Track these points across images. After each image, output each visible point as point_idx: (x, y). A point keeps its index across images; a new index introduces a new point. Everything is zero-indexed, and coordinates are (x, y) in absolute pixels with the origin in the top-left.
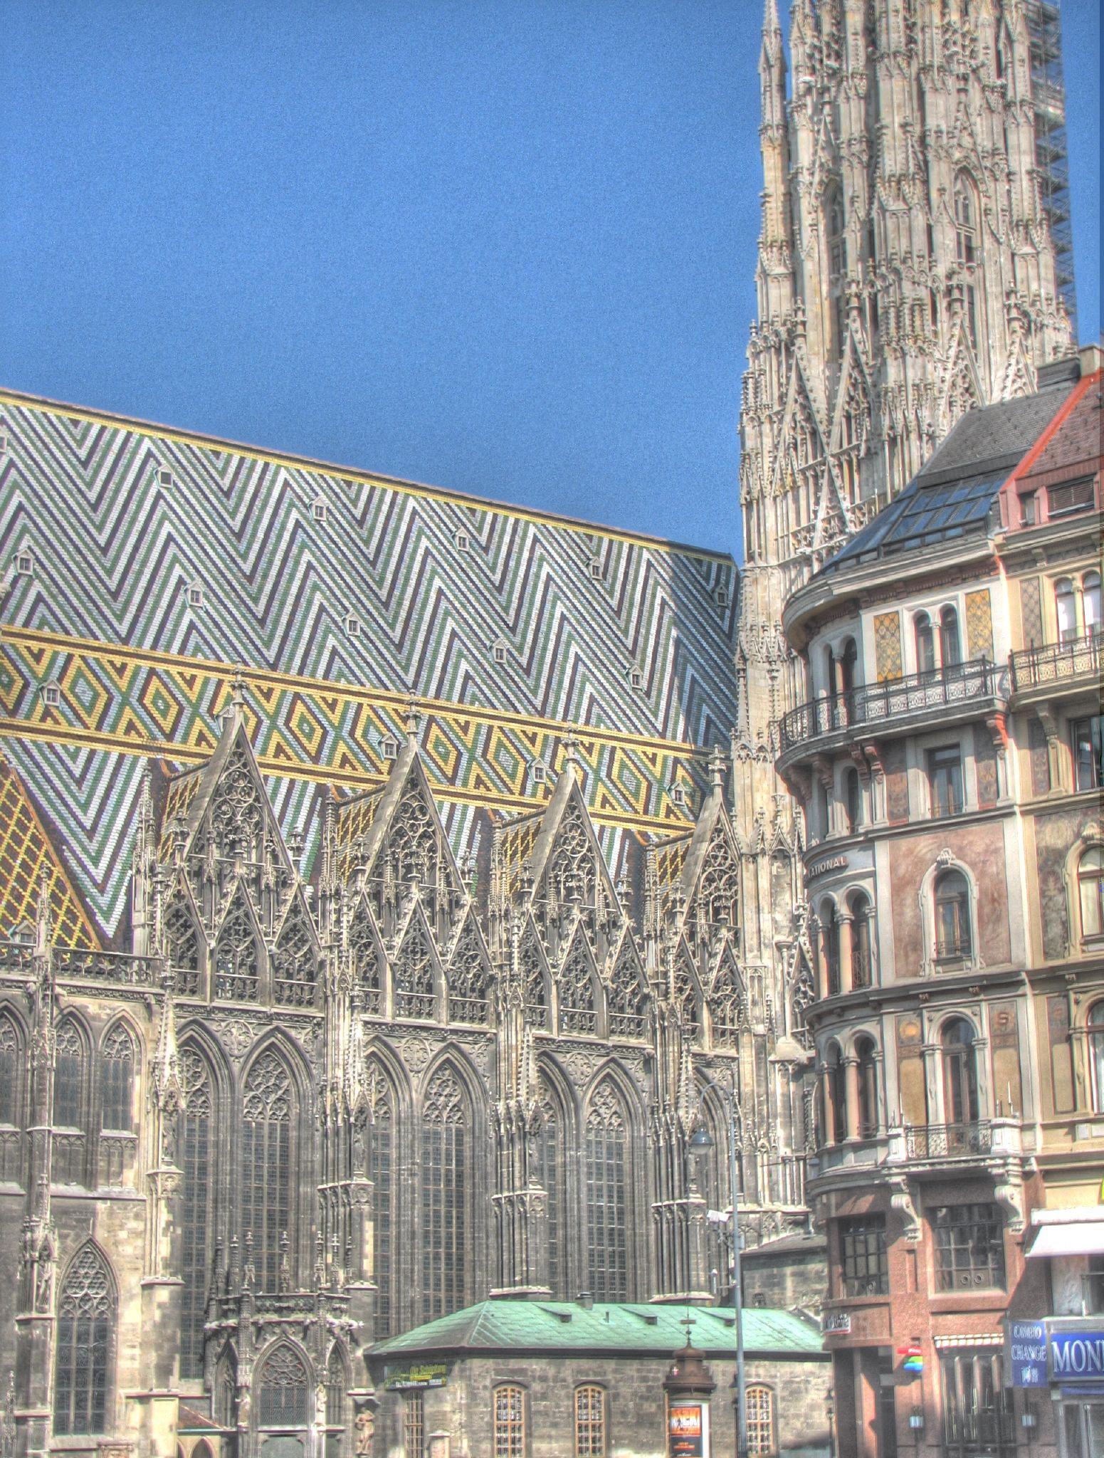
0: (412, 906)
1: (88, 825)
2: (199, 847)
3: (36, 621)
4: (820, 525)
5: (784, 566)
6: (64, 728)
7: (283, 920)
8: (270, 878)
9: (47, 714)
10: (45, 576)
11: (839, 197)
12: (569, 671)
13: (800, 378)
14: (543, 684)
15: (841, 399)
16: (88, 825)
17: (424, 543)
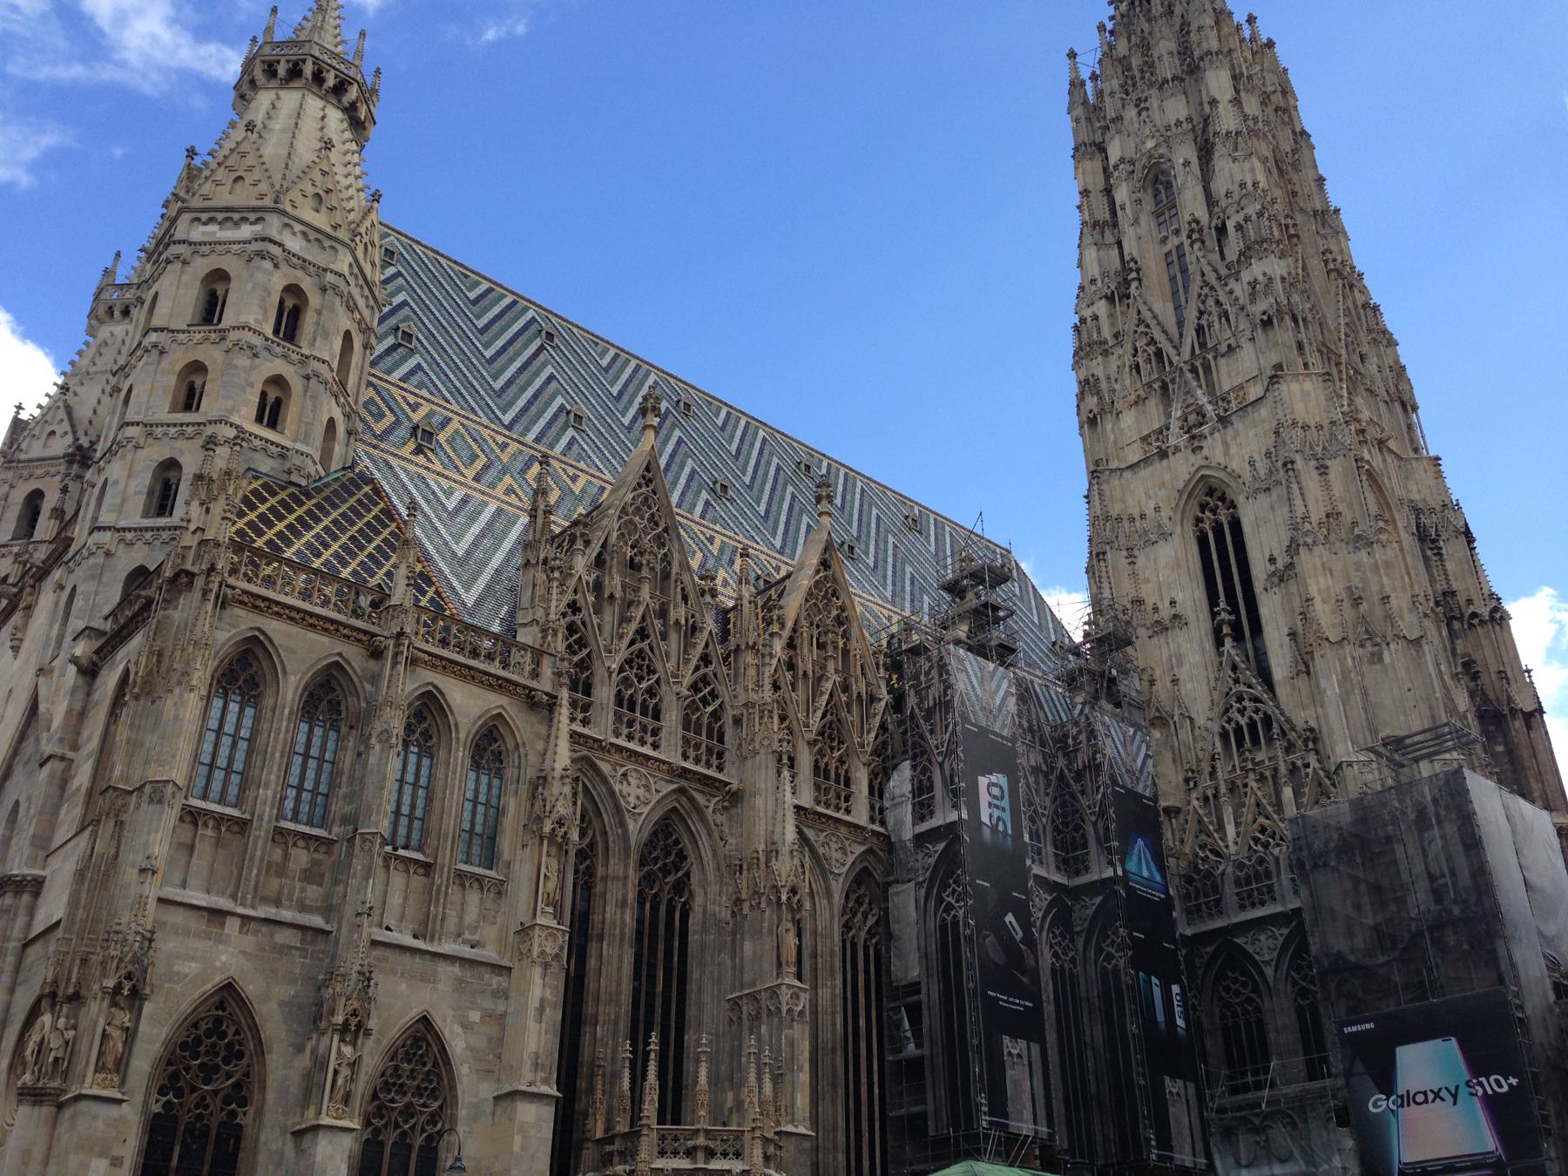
0: (829, 685)
1: (460, 553)
2: (600, 562)
3: (415, 380)
4: (1175, 425)
5: (1131, 467)
6: (438, 467)
7: (694, 662)
8: (679, 613)
9: (419, 450)
10: (426, 355)
11: (1162, 178)
12: (908, 582)
13: (1139, 312)
14: (889, 581)
15: (1191, 314)
16: (460, 553)
17: (775, 460)
